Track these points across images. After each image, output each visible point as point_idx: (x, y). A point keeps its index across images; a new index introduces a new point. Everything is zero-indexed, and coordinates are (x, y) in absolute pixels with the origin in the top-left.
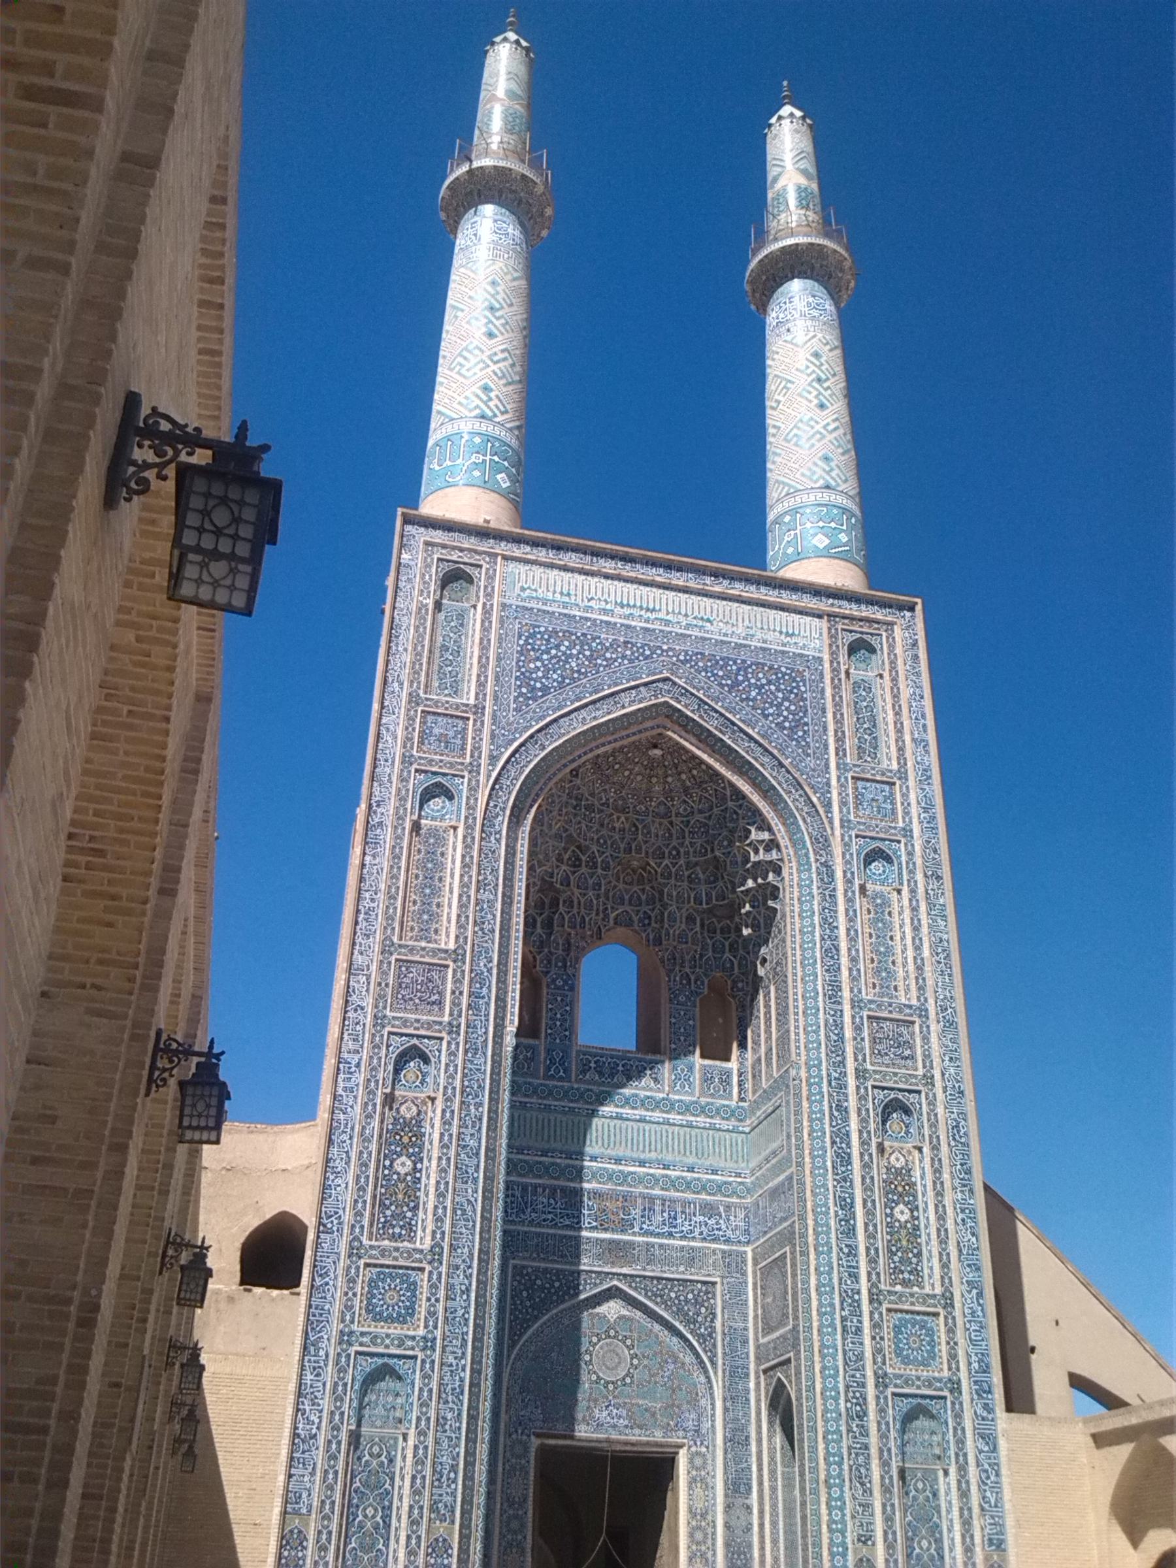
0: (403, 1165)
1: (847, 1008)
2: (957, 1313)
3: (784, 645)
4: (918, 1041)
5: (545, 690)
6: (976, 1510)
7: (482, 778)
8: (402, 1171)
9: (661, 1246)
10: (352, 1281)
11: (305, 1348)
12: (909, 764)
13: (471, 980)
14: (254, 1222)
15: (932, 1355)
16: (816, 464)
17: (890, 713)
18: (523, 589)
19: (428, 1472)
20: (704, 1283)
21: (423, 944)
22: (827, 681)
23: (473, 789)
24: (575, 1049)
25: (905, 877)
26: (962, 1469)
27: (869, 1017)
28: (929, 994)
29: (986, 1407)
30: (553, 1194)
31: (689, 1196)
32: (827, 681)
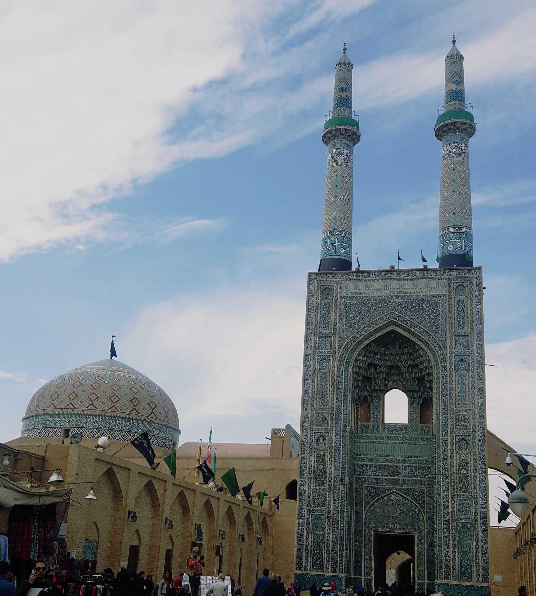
0: (321, 467)
1: (449, 412)
2: (478, 500)
3: (433, 293)
4: (471, 420)
5: (354, 323)
6: (480, 553)
7: (336, 355)
8: (321, 468)
9: (408, 480)
10: (309, 497)
11: (299, 514)
12: (475, 328)
13: (336, 415)
14: (289, 482)
15: (470, 512)
16: (451, 217)
17: (469, 310)
18: (347, 290)
19: (331, 543)
20: (421, 489)
21: (323, 407)
22: (447, 303)
23: (334, 359)
24: (381, 424)
25: (471, 368)
26: (477, 542)
27: (456, 414)
28: (476, 405)
29: (485, 526)
30: (375, 467)
31: (417, 465)
32: (447, 303)
